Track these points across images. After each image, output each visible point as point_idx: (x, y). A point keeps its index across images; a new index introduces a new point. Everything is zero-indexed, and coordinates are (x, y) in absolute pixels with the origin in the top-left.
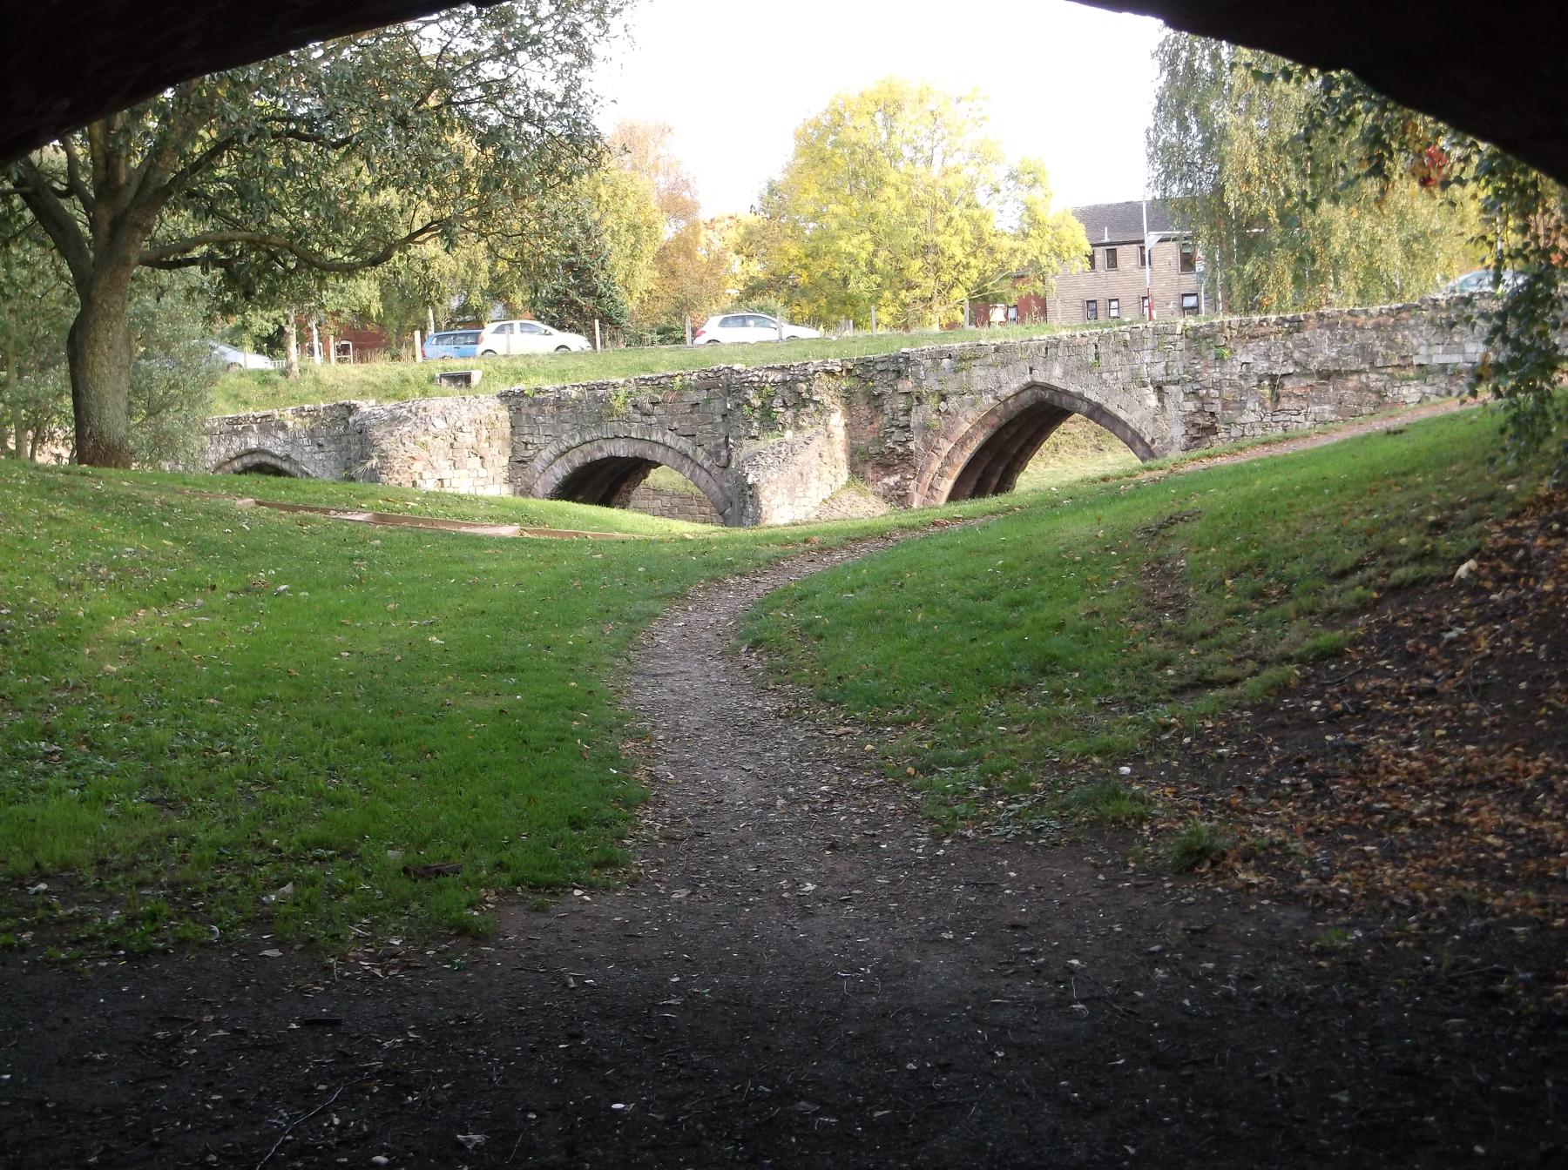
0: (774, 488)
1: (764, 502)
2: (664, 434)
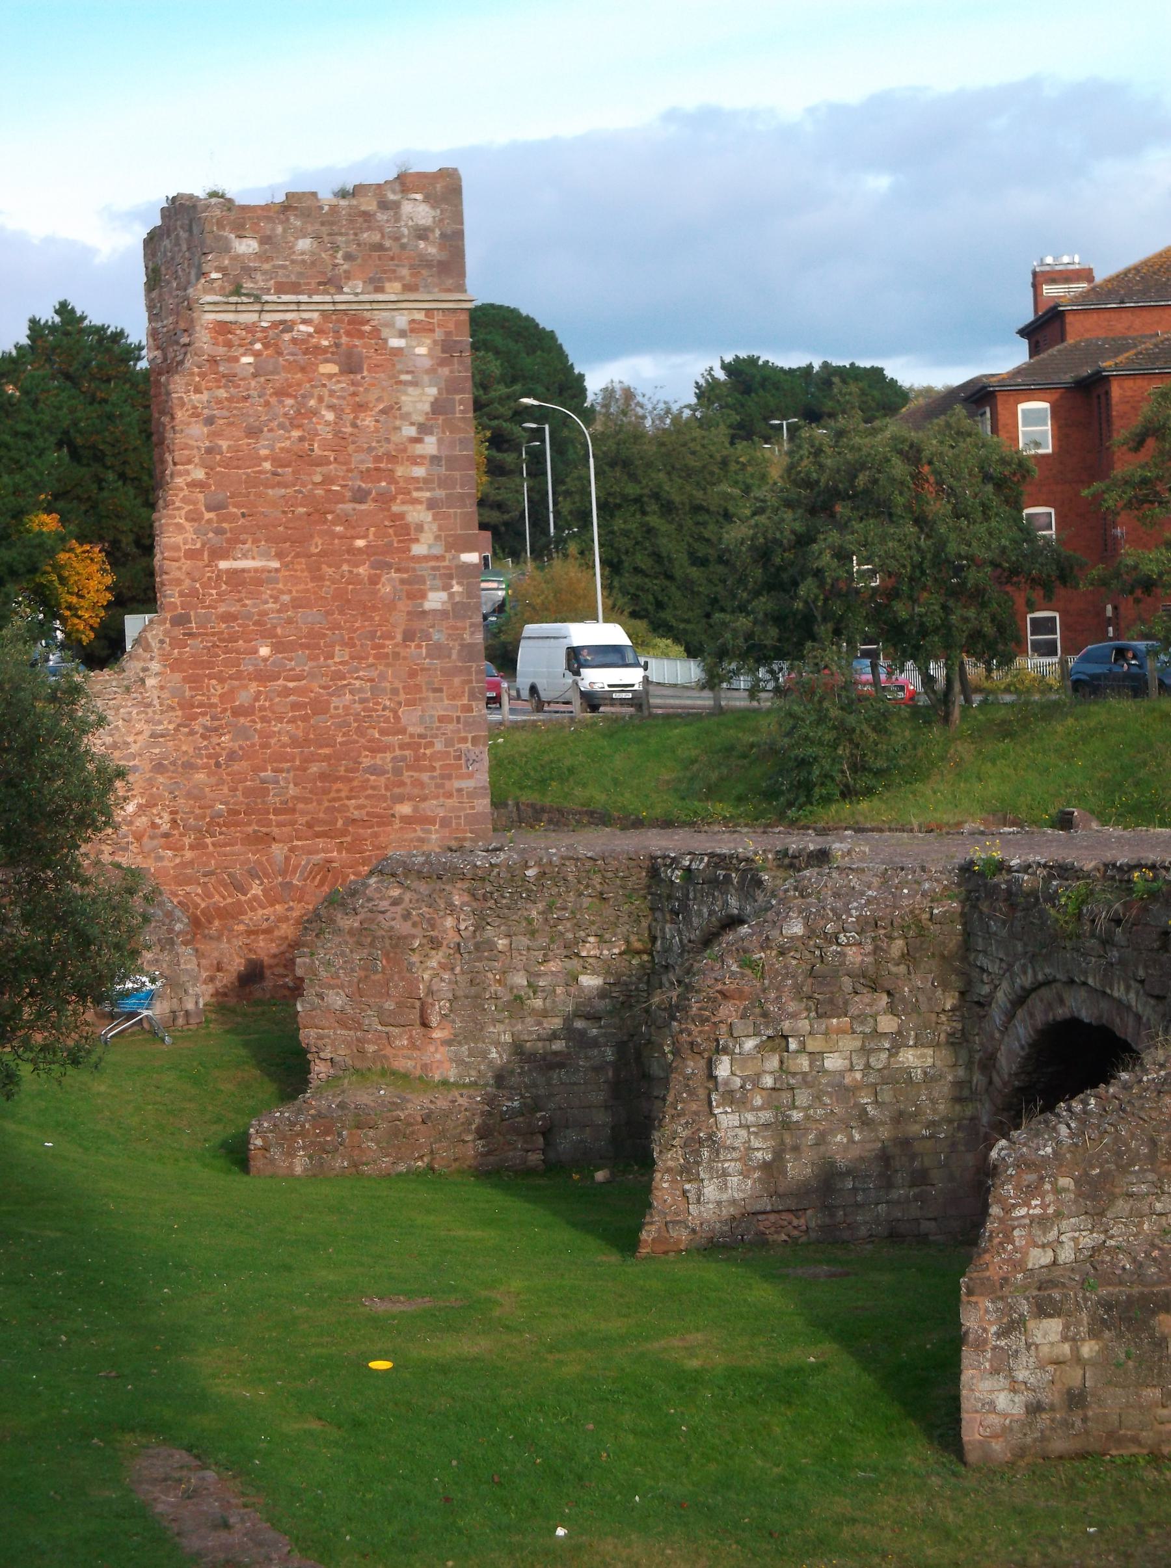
0: (1030, 1177)
1: (995, 1210)
2: (1128, 988)
